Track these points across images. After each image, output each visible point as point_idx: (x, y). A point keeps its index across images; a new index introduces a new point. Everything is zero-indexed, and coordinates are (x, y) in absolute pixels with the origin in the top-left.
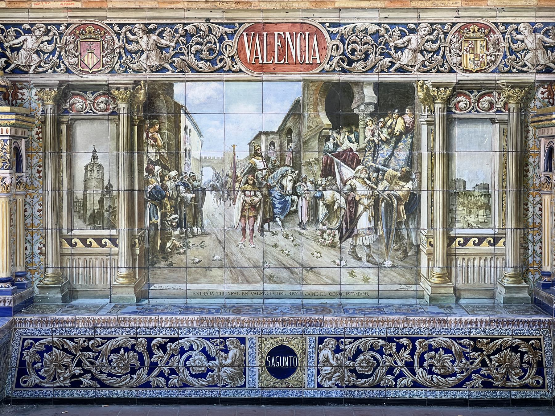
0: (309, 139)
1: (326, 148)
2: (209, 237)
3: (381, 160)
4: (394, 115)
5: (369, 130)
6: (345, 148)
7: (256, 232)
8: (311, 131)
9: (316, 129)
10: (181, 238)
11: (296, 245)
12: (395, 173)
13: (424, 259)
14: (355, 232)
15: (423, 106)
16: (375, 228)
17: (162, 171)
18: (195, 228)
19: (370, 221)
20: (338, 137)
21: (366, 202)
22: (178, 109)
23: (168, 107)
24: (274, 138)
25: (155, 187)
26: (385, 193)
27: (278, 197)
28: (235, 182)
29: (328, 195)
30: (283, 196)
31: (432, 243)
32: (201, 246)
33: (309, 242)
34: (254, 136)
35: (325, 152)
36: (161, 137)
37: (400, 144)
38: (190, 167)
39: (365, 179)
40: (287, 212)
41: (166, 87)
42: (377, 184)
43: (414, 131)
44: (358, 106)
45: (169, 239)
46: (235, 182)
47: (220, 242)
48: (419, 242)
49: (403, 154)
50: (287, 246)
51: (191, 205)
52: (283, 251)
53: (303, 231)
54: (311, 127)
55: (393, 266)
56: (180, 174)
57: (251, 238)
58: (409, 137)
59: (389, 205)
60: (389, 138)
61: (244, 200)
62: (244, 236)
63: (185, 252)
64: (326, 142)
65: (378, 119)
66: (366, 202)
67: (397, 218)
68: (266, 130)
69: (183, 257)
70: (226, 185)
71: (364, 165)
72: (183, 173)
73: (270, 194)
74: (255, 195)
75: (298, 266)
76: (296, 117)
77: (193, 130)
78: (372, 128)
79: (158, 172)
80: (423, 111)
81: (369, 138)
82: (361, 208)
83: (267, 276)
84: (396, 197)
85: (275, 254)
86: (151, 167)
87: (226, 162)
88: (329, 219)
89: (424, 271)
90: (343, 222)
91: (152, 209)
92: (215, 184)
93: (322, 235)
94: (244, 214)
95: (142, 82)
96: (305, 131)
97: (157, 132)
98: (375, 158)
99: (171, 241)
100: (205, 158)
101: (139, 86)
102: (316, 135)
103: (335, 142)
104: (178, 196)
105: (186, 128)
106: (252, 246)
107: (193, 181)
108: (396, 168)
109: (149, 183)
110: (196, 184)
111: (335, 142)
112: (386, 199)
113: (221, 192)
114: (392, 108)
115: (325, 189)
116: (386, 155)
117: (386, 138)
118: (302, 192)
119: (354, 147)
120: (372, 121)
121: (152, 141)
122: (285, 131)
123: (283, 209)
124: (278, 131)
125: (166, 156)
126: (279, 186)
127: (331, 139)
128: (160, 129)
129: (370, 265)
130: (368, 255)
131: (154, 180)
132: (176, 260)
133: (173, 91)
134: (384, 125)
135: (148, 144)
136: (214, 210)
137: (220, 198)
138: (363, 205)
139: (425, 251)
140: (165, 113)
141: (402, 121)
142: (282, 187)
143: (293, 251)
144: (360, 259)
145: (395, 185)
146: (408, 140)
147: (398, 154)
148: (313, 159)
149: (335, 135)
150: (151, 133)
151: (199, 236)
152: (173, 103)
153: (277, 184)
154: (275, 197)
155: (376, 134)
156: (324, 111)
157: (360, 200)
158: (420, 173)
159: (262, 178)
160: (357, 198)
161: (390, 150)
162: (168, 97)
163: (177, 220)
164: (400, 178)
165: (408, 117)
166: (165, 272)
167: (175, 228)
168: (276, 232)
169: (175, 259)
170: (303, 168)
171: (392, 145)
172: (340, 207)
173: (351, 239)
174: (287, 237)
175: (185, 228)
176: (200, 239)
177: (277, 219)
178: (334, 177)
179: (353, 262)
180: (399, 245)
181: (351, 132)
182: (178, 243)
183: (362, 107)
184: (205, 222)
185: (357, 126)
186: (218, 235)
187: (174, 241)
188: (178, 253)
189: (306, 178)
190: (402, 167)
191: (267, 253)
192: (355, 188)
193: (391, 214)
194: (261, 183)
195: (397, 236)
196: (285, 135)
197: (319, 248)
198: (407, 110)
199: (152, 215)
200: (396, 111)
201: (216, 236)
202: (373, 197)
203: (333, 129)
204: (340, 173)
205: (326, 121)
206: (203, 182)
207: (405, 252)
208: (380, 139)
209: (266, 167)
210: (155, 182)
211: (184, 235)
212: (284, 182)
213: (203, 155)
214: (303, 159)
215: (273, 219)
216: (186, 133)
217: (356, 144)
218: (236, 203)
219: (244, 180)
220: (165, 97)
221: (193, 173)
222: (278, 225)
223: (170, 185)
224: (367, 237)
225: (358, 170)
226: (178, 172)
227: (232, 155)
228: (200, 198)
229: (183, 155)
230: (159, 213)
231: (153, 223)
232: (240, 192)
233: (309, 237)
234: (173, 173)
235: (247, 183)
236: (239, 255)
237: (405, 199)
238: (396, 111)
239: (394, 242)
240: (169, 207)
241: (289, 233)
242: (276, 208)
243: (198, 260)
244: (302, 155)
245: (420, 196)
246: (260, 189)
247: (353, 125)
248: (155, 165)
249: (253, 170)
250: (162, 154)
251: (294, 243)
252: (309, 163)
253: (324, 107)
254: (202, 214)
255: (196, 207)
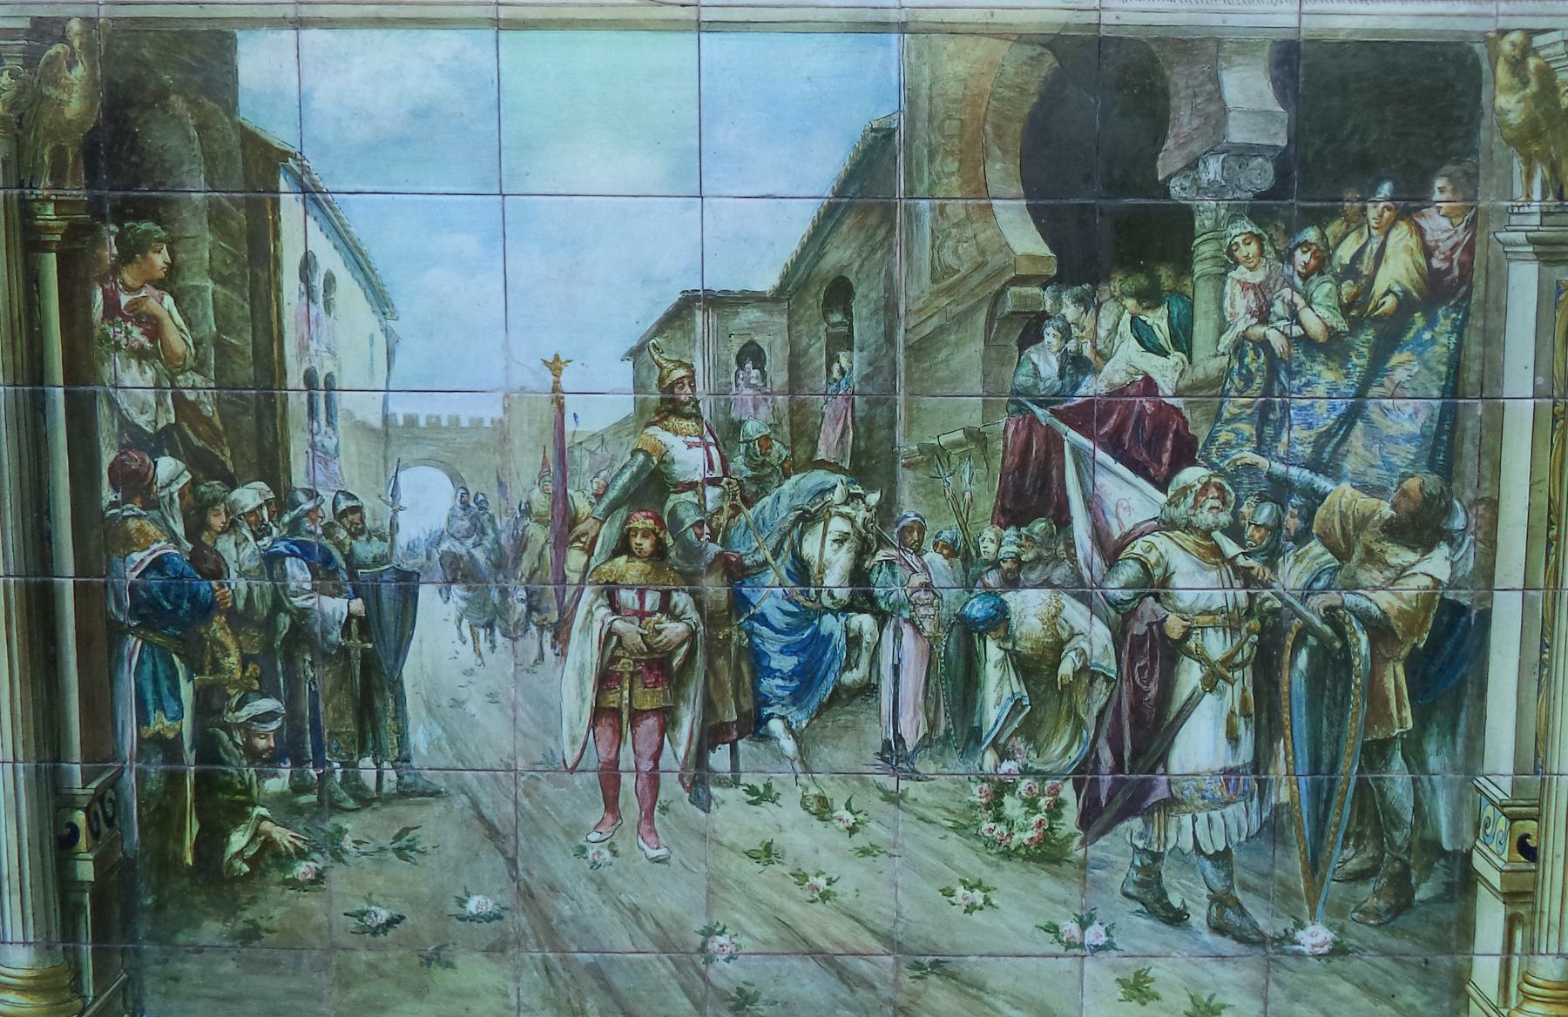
0: (941, 330)
1: (1024, 379)
2: (438, 807)
3: (1299, 438)
4: (1372, 213)
5: (1245, 286)
6: (1120, 379)
7: (671, 787)
8: (949, 290)
9: (976, 279)
10: (299, 810)
11: (864, 852)
12: (1365, 503)
13: (1490, 918)
14: (1160, 793)
15: (1518, 166)
16: (1259, 764)
17: (194, 483)
18: (368, 761)
19: (1233, 738)
20: (1088, 322)
21: (1216, 645)
22: (260, 167)
23: (210, 160)
24: (758, 327)
25: (158, 564)
26: (1317, 601)
27: (778, 620)
28: (562, 543)
29: (1030, 608)
30: (807, 616)
31: (1532, 843)
32: (399, 852)
33: (932, 837)
34: (659, 314)
35: (1020, 401)
36: (182, 313)
37: (1396, 359)
38: (334, 467)
39: (1217, 535)
40: (825, 691)
41: (198, 52)
42: (1272, 555)
43: (1468, 295)
44: (1193, 165)
45: (238, 813)
46: (562, 543)
47: (493, 832)
48: (1470, 839)
49: (1409, 406)
50: (824, 854)
51: (344, 652)
52: (801, 877)
53: (903, 785)
54: (950, 271)
55: (1338, 950)
56: (282, 500)
57: (649, 816)
58: (1444, 325)
59: (1332, 665)
60: (1342, 326)
61: (610, 633)
62: (611, 804)
63: (320, 877)
64: (1023, 345)
65: (1289, 233)
66: (1216, 645)
67: (1368, 726)
68: (718, 281)
69: (309, 901)
70: (517, 561)
71: (1211, 465)
72: (301, 497)
73: (739, 603)
74: (666, 607)
75: (876, 946)
76: (873, 220)
77: (346, 282)
78: (1258, 277)
79: (175, 488)
80: (1518, 190)
81: (1241, 327)
82: (1190, 676)
83: (723, 996)
84: (1366, 619)
85: (760, 890)
86: (136, 459)
87: (517, 441)
88: (1031, 730)
89: (1485, 973)
90: (1102, 742)
91: (148, 668)
92: (460, 549)
93: (995, 805)
94: (612, 700)
95: (75, 26)
96: (915, 290)
97: (160, 285)
98: (1269, 431)
99: (252, 822)
100: (411, 421)
101: (58, 48)
102: (973, 309)
103: (1071, 346)
104: (278, 606)
105: (307, 265)
106: (653, 853)
107: (354, 536)
108: (1372, 477)
109: (129, 544)
110: (366, 549)
111: (1071, 346)
112: (1317, 633)
113: (495, 595)
114: (1365, 171)
115: (1012, 583)
116: (1325, 416)
117: (1329, 329)
118: (899, 594)
119: (1165, 371)
120: (1259, 238)
121: (136, 332)
122: (816, 289)
123: (806, 679)
124: (781, 290)
125: (209, 409)
126: (784, 562)
127: (1051, 335)
128: (173, 269)
129: (1227, 945)
130: (1220, 900)
131: (152, 529)
132: (277, 913)
133: (233, 72)
134: (1322, 263)
135: (117, 347)
136: (463, 680)
137: (488, 618)
138: (1202, 658)
139: (1495, 879)
140: (196, 191)
141: (1413, 242)
142: (802, 572)
143: (852, 877)
144: (1177, 919)
145: (1362, 562)
146: (1437, 336)
147: (1385, 411)
148: (959, 435)
149: (1070, 311)
150: (129, 290)
151: (387, 800)
152: (235, 139)
153: (776, 553)
154: (763, 619)
155: (1279, 308)
156: (1017, 189)
157: (1187, 635)
158: (1493, 505)
159: (699, 524)
160: (1174, 627)
161: (1347, 386)
162: (210, 105)
163: (274, 726)
164: (1395, 531)
165: (1445, 223)
166: (222, 970)
167: (271, 761)
168: (768, 787)
169: (274, 907)
170: (907, 481)
171: (1359, 362)
172: (1086, 672)
173: (1136, 824)
174: (822, 810)
175: (319, 762)
176: (394, 818)
177: (776, 726)
178: (1063, 520)
179: (1141, 931)
180: (1370, 852)
181: (1150, 297)
182: (283, 836)
183: (1213, 169)
184: (419, 738)
185: (1184, 264)
186: (485, 800)
187: (266, 825)
188: (286, 883)
189: (922, 530)
190: (1404, 476)
191: (725, 888)
192: (1166, 580)
193: (1342, 704)
194: (691, 553)
195: (1362, 812)
196: (817, 312)
197: (978, 863)
198: (1440, 183)
199: (149, 696)
200: (1386, 189)
201: (475, 805)
202: (1254, 623)
203: (1062, 279)
204: (1092, 503)
205: (1025, 240)
206: (402, 539)
207: (1401, 886)
208: (1297, 330)
209: (718, 473)
210: (154, 542)
211: (313, 798)
212: (810, 548)
213: (401, 408)
214: (909, 429)
215: (754, 725)
216: (309, 293)
217: (1177, 357)
218: (573, 647)
219: (608, 534)
220: (194, 104)
221: (355, 498)
222: (780, 755)
223: (238, 553)
224: (1216, 815)
225: (1184, 491)
226: (273, 484)
227: (549, 410)
228: (389, 617)
229: (297, 402)
230: (186, 690)
231: (159, 740)
232: (588, 594)
233: (930, 814)
234: (249, 496)
235: (623, 547)
236: (589, 896)
237: (1409, 632)
238: (1386, 189)
239: (1346, 837)
240: (232, 661)
241: (837, 793)
242: (771, 673)
243: (384, 915)
244: (901, 411)
245: (1485, 617)
246: (689, 580)
247: (1163, 259)
248: (156, 453)
249: (654, 483)
250: (191, 396)
251: (860, 840)
252: (936, 455)
253: (1014, 169)
254: (400, 699)
255: (370, 663)
